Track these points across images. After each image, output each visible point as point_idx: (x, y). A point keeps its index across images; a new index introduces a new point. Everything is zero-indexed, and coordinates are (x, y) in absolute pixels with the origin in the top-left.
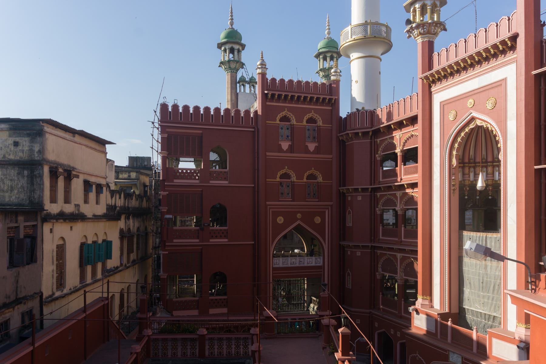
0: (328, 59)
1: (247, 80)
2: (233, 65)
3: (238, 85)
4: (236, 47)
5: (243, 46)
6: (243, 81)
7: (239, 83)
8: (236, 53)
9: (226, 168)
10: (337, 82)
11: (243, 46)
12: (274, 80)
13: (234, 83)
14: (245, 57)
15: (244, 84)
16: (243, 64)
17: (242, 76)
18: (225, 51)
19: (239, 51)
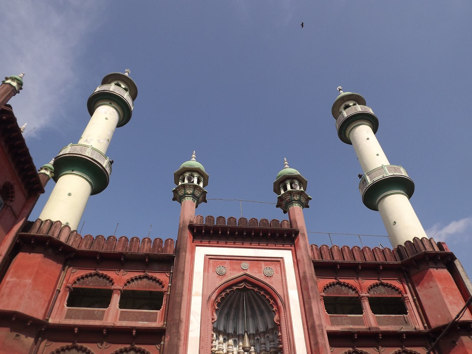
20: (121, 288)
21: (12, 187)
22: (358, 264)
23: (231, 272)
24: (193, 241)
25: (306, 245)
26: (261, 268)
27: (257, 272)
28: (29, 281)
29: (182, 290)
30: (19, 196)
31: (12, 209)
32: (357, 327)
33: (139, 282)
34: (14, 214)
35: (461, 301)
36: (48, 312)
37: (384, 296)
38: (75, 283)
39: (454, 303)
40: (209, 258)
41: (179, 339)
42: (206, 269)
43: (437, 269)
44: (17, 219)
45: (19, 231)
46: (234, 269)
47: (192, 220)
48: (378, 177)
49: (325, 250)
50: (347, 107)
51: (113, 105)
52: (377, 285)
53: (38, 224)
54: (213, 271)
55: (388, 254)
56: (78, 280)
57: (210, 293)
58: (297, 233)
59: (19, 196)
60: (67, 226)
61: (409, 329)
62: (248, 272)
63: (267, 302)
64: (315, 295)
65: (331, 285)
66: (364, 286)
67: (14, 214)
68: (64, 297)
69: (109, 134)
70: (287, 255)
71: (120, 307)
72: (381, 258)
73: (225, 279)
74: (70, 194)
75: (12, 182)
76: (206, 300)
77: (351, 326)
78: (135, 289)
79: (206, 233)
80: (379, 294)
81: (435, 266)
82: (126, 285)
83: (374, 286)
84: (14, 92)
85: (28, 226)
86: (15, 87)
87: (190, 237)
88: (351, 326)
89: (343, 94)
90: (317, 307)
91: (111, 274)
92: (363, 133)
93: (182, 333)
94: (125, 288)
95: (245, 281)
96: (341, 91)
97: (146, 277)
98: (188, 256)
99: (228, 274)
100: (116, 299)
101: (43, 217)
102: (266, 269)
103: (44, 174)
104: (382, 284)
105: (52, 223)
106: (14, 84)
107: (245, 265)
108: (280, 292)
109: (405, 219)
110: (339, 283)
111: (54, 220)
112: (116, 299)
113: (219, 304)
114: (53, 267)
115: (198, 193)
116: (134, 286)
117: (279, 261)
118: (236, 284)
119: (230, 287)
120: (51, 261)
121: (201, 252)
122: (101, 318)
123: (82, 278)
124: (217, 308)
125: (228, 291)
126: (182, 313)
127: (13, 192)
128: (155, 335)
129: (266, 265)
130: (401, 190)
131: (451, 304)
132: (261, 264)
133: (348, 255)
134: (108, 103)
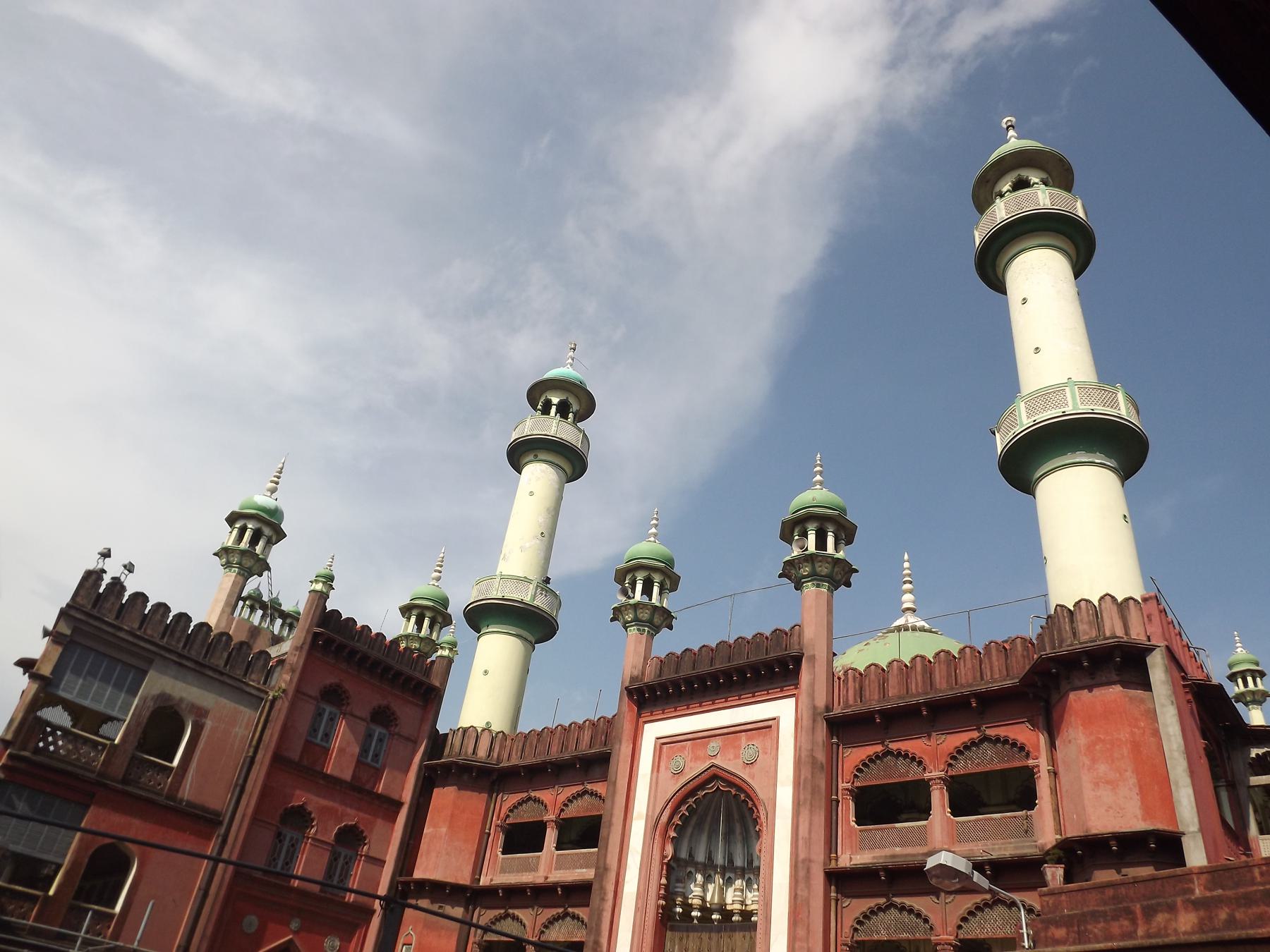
0: (426, 622)
1: (265, 598)
2: (248, 563)
3: (241, 603)
4: (267, 531)
5: (281, 535)
6: (256, 601)
7: (244, 599)
8: (261, 543)
9: (171, 761)
10: (449, 661)
11: (281, 535)
12: (336, 613)
13: (237, 597)
14: (277, 555)
15: (257, 606)
16: (269, 569)
17: (258, 589)
18: (243, 531)
19: (270, 543)
20: (553, 817)
21: (388, 707)
22: (918, 705)
23: (692, 765)
24: (639, 715)
25: (812, 685)
26: (739, 747)
27: (732, 756)
28: (444, 830)
29: (612, 815)
30: (407, 713)
31: (401, 736)
32: (909, 850)
33: (579, 802)
34: (408, 739)
35: (1129, 774)
36: (478, 868)
37: (988, 768)
38: (508, 816)
39: (1108, 782)
40: (664, 743)
41: (603, 899)
42: (656, 767)
43: (1090, 691)
44: (415, 743)
45: (422, 760)
46: (696, 759)
47: (636, 673)
48: (1049, 414)
49: (873, 677)
50: (1021, 184)
51: (541, 456)
52: (973, 743)
53: (450, 737)
54: (667, 768)
55: (1019, 654)
56: (511, 811)
57: (658, 811)
58: (798, 660)
59: (407, 713)
60: (487, 729)
61: (1023, 847)
62: (717, 762)
63: (747, 814)
64: (809, 797)
65: (872, 760)
66: (933, 755)
67: (408, 739)
68: (497, 841)
69: (541, 520)
70: (782, 710)
71: (557, 849)
72: (996, 669)
73: (683, 780)
74: (486, 672)
75: (385, 703)
76: (653, 827)
77: (898, 850)
78: (574, 815)
79: (654, 694)
80: (978, 764)
81: (1088, 681)
82: (562, 810)
83: (967, 748)
84: (323, 596)
85: (438, 742)
86: (321, 592)
87: (631, 710)
88: (898, 850)
89: (1014, 143)
90: (807, 824)
91: (546, 795)
92: (1039, 275)
93: (610, 888)
94: (563, 816)
95: (715, 777)
96: (1011, 133)
97: (585, 792)
98: (625, 749)
99: (686, 770)
100: (551, 836)
101: (465, 722)
102: (749, 747)
103: (441, 657)
104: (986, 739)
105: (465, 730)
106: (319, 587)
107: (714, 745)
108: (761, 794)
109: (1086, 539)
110: (888, 753)
111: (466, 725)
112: (551, 836)
113: (679, 829)
114: (475, 801)
115: (645, 615)
116: (572, 811)
117: (767, 727)
118: (702, 786)
119: (692, 793)
120: (469, 793)
121: (653, 731)
122: (535, 869)
123: (515, 807)
124: (673, 834)
125: (691, 800)
126: (609, 856)
127: (393, 714)
128: (579, 893)
129: (749, 739)
130: (1074, 451)
131: (1097, 785)
132: (740, 739)
133: (919, 678)
134: (531, 457)
